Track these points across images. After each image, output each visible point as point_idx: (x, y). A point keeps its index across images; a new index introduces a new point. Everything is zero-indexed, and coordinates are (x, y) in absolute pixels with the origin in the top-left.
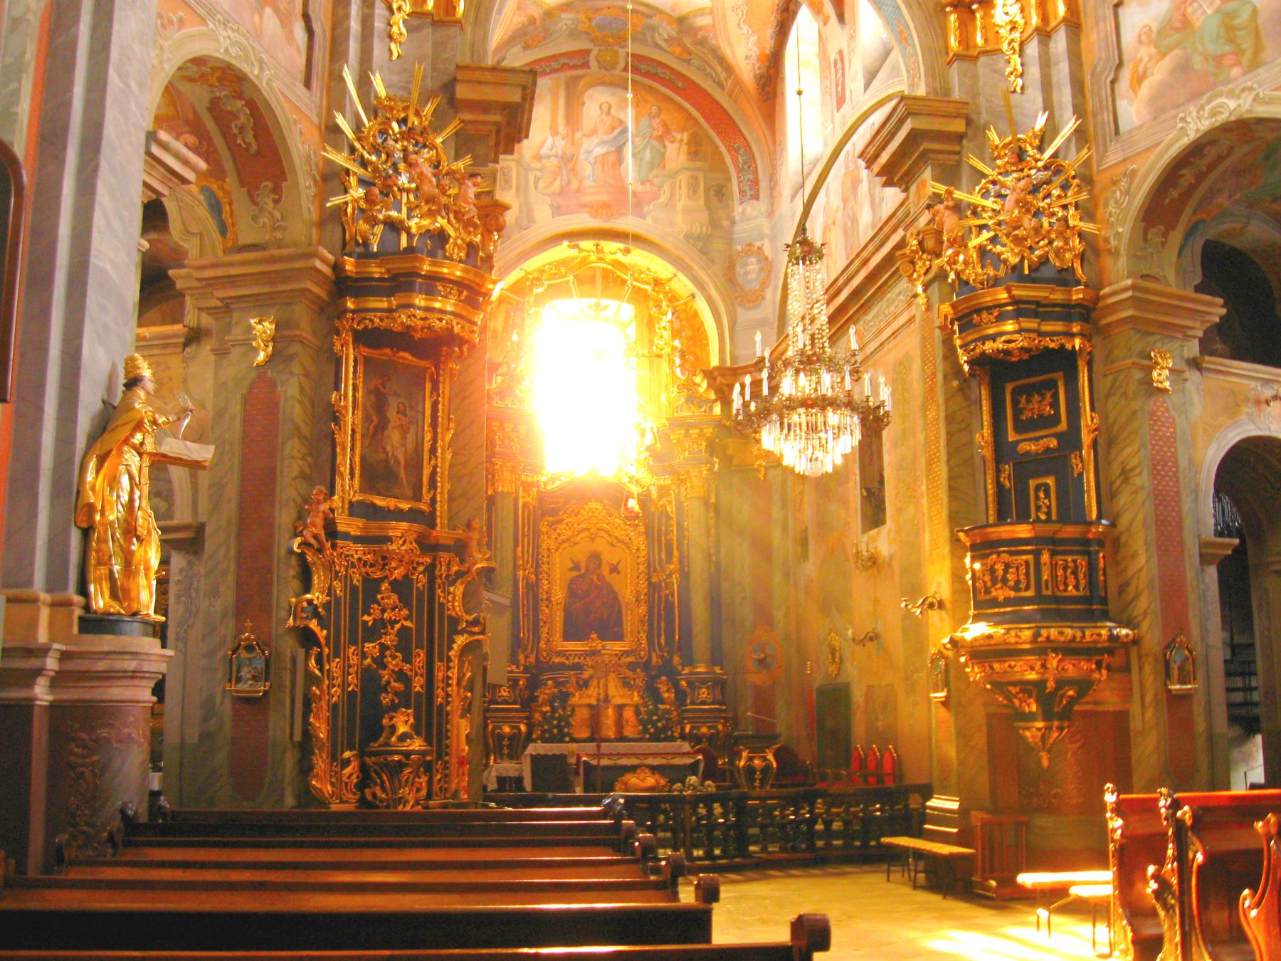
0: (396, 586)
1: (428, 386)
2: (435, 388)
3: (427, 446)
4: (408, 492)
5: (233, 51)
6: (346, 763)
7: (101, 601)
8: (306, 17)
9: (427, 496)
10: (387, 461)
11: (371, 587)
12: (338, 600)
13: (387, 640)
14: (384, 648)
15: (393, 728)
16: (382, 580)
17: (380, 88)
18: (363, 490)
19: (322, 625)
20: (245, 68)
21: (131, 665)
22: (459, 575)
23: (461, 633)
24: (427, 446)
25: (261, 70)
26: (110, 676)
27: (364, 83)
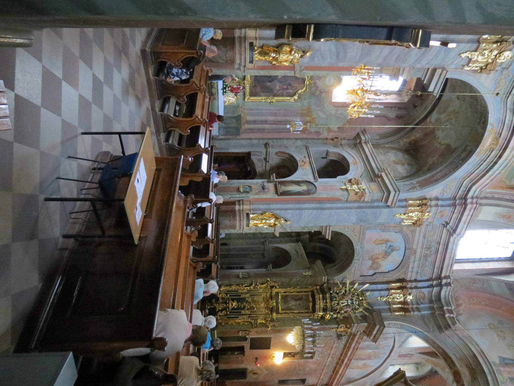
2: (306, 313)
6: (227, 294)
7: (251, 216)
8: (375, 273)
15: (234, 302)
17: (368, 294)
20: (355, 255)
21: (242, 219)
27: (367, 290)
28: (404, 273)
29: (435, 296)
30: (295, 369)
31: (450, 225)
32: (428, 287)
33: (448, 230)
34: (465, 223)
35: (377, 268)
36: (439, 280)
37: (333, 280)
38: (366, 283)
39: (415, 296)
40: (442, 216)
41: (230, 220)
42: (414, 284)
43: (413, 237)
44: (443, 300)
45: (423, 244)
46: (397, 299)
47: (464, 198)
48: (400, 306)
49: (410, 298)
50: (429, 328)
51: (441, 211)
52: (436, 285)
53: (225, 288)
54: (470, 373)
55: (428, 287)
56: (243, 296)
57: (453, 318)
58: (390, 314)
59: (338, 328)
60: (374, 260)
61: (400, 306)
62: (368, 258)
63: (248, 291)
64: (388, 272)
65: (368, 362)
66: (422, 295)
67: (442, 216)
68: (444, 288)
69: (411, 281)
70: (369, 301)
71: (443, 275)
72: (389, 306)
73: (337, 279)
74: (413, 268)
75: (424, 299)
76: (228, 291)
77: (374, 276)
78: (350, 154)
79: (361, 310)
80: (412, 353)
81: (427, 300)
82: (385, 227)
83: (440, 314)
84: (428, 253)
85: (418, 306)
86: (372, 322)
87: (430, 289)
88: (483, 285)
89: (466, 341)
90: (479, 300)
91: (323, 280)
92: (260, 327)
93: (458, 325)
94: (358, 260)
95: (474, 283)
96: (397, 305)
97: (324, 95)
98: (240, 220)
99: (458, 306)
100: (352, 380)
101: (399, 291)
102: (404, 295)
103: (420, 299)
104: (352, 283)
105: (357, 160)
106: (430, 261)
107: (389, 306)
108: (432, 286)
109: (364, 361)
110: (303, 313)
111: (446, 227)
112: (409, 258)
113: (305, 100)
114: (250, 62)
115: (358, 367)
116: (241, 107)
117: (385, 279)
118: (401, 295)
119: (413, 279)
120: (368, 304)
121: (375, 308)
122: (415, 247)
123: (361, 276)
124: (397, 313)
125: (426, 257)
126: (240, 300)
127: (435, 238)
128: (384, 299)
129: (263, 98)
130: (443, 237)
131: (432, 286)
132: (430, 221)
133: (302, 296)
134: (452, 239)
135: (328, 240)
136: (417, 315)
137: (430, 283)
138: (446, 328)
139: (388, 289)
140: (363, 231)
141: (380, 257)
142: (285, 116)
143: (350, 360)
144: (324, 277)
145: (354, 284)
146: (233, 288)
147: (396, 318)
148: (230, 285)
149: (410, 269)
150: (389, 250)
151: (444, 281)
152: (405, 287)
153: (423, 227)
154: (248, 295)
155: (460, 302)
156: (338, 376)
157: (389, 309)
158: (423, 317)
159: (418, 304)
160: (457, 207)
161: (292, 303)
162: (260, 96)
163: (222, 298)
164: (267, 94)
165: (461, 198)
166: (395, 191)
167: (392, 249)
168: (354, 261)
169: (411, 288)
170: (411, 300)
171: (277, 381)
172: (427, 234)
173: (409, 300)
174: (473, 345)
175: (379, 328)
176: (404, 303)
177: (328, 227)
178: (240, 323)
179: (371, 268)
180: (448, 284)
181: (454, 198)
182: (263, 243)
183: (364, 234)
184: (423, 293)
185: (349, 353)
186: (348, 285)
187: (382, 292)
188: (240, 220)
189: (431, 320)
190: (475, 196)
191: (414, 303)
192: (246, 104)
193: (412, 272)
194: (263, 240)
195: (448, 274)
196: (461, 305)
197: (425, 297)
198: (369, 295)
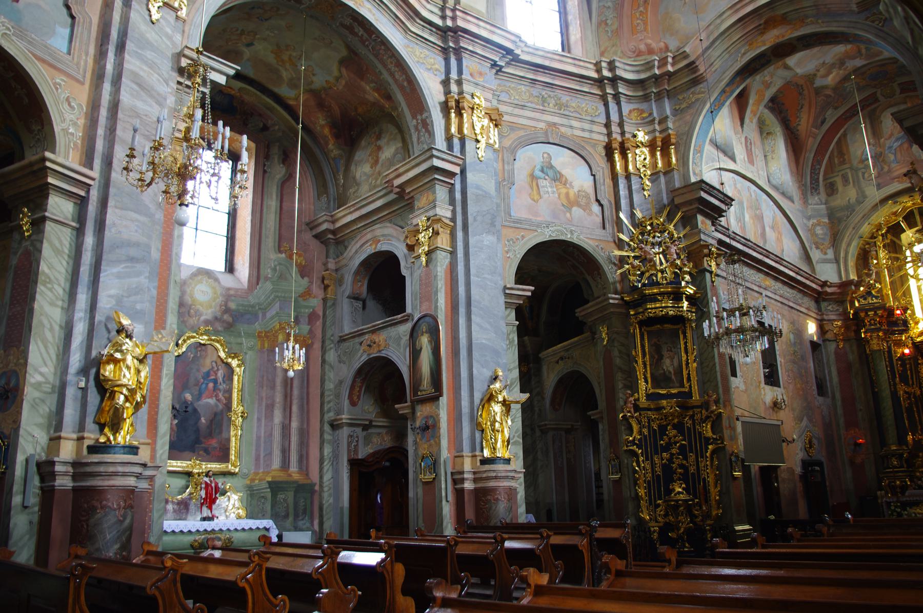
0: (674, 427)
1: (682, 337)
2: (685, 337)
3: (684, 363)
4: (678, 385)
5: (554, 235)
6: (658, 506)
7: (487, 453)
8: (598, 201)
9: (687, 385)
10: (664, 373)
11: (663, 429)
12: (645, 436)
13: (674, 451)
14: (672, 455)
15: (674, 490)
16: (668, 425)
17: (639, 214)
18: (653, 388)
19: (639, 447)
20: (563, 238)
21: (494, 474)
22: (708, 417)
23: (711, 444)
24: (684, 363)
25: (572, 234)
26: (488, 479)
27: (632, 216)
28: (594, 146)
29: (634, 91)
30: (794, 362)
31: (497, 59)
32: (618, 103)
33: (508, 64)
34: (493, 32)
35: (587, 196)
36: (605, 84)
37: (614, 283)
38: (618, 218)
39: (638, 126)
40: (481, 74)
41: (497, 499)
42: (615, 129)
43: (523, 127)
44: (643, 76)
45: (534, 110)
46: (645, 159)
47: (445, 32)
48: (658, 153)
49: (642, 136)
50: (697, 100)
51: (471, 75)
52: (615, 87)
53: (644, 509)
54: (775, 27)
55: (618, 103)
56: (658, 470)
57: (673, 58)
58: (675, 172)
59: (711, 272)
60: (571, 203)
61: (658, 153)
62: (568, 215)
63: (647, 459)
64: (594, 176)
65: (768, 221)
66: (635, 114)
67: (481, 74)
68: (619, 72)
69: (609, 134)
70: (654, 211)
71: (595, 75)
72: (661, 175)
73: (613, 274)
74: (583, 130)
75: (642, 111)
76: (650, 504)
77: (602, 202)
78: (356, 252)
79: (671, 227)
80: (743, 140)
81: (644, 106)
82: (504, 180)
83: (669, 80)
84: (552, 102)
85: (657, 122)
86: (694, 206)
87: (623, 99)
88: (609, 7)
89: (716, 34)
90: (638, 15)
91: (616, 302)
92: (721, 431)
93: (687, 49)
94: (571, 232)
95: (606, 24)
96: (656, 159)
97: (233, 306)
98: (496, 478)
99: (651, 51)
100: (802, 252)
101: (630, 155)
102: (638, 146)
103: (644, 118)
104: (620, 244)
105: (369, 236)
106: (568, 98)
107: (661, 175)
108: (616, 96)
109: (767, 229)
110: (686, 343)
111: (501, 67)
112: (563, 136)
113: (241, 344)
114: (136, 454)
115: (779, 240)
116: (253, 480)
117: (609, 182)
118: (638, 151)
119: (605, 131)
120: (659, 212)
121: (665, 201)
122: (542, 125)
123: (604, 228)
124: (674, 160)
125: (560, 105)
126: (669, 474)
127: (523, 88)
128: (648, 183)
129: (232, 433)
130: (522, 74)
131: (616, 96)
132: (490, 96)
133: (650, 345)
134: (524, 57)
135: (533, 292)
136: (674, 123)
137: (610, 98)
138: (695, 70)
139: (628, 177)
140: (514, 222)
141: (564, 191)
142: (273, 387)
143: (768, 254)
144: (611, 301)
145: (620, 240)
146: (642, 492)
147: (684, 160)
148: (637, 498)
149: (586, 135)
150: (550, 173)
151: (606, 73)
152: (622, 144)
153: (503, 108)
154: (656, 460)
155: (642, 47)
156: (799, 278)
157: (665, 174)
158: (675, 112)
159: (654, 120)
160: (462, 45)
161: (668, 365)
162: (228, 440)
163: (666, 515)
164: (225, 424)
165: (444, 39)
166: (432, 156)
167: (547, 167)
168: (575, 241)
169: (623, 133)
170: (646, 134)
171: (821, 399)
172: (516, 102)
173: (647, 138)
174: (722, 22)
175: (705, 192)
176: (652, 146)
177: (507, 291)
178: (716, 475)
179: (586, 208)
180: (612, 66)
181: (445, 51)
182: (544, 432)
183: (519, 221)
184: (630, 111)
185: (755, 254)
186: (625, 254)
187: (634, 188)
188: (496, 478)
189: (681, 98)
190: (440, 13)
191: (650, 128)
192: (245, 471)
193: (591, 131)
194: (538, 433)
195: (591, 66)
196: (647, 45)
197: (638, 109)
198: (642, 212)
